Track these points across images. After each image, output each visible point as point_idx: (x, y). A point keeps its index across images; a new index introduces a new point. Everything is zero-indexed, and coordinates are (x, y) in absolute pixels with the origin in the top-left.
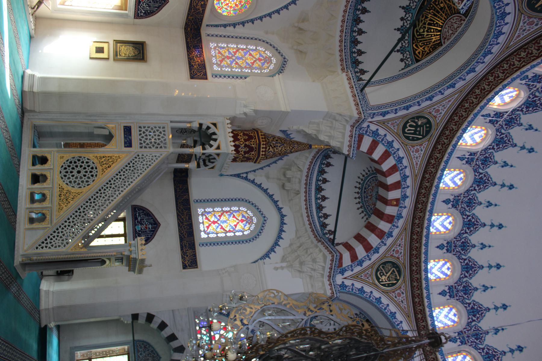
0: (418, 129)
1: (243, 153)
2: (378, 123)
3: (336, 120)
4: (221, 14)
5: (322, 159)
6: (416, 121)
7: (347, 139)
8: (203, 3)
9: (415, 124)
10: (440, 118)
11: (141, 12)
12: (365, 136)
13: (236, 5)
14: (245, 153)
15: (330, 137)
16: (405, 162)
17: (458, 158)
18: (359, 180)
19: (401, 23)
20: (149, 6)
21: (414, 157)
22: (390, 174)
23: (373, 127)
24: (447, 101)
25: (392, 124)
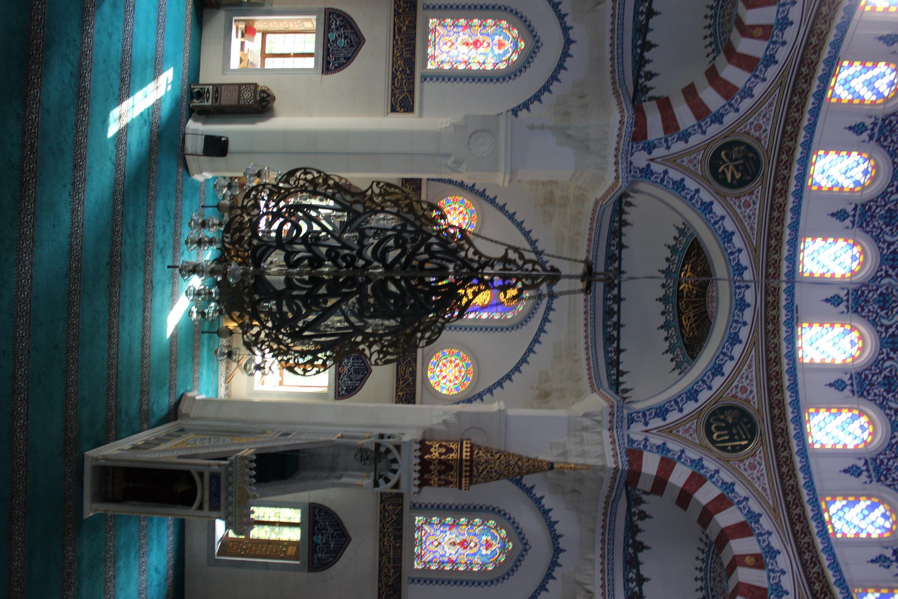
0: (734, 431)
1: (437, 454)
2: (660, 430)
3: (585, 429)
4: (440, 393)
5: (626, 572)
6: (722, 417)
7: (608, 448)
8: (411, 369)
9: (723, 425)
10: (756, 400)
11: (342, 389)
12: (645, 454)
13: (456, 377)
14: (441, 454)
15: (583, 454)
16: (741, 490)
17: (846, 471)
18: (700, 584)
19: (668, 343)
20: (351, 380)
21: (753, 478)
22: (720, 511)
23: (656, 440)
24: (746, 366)
25: (686, 431)
